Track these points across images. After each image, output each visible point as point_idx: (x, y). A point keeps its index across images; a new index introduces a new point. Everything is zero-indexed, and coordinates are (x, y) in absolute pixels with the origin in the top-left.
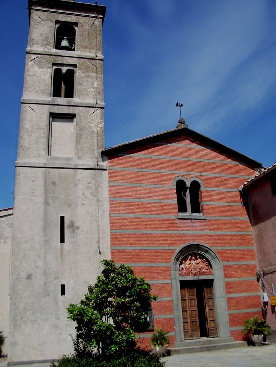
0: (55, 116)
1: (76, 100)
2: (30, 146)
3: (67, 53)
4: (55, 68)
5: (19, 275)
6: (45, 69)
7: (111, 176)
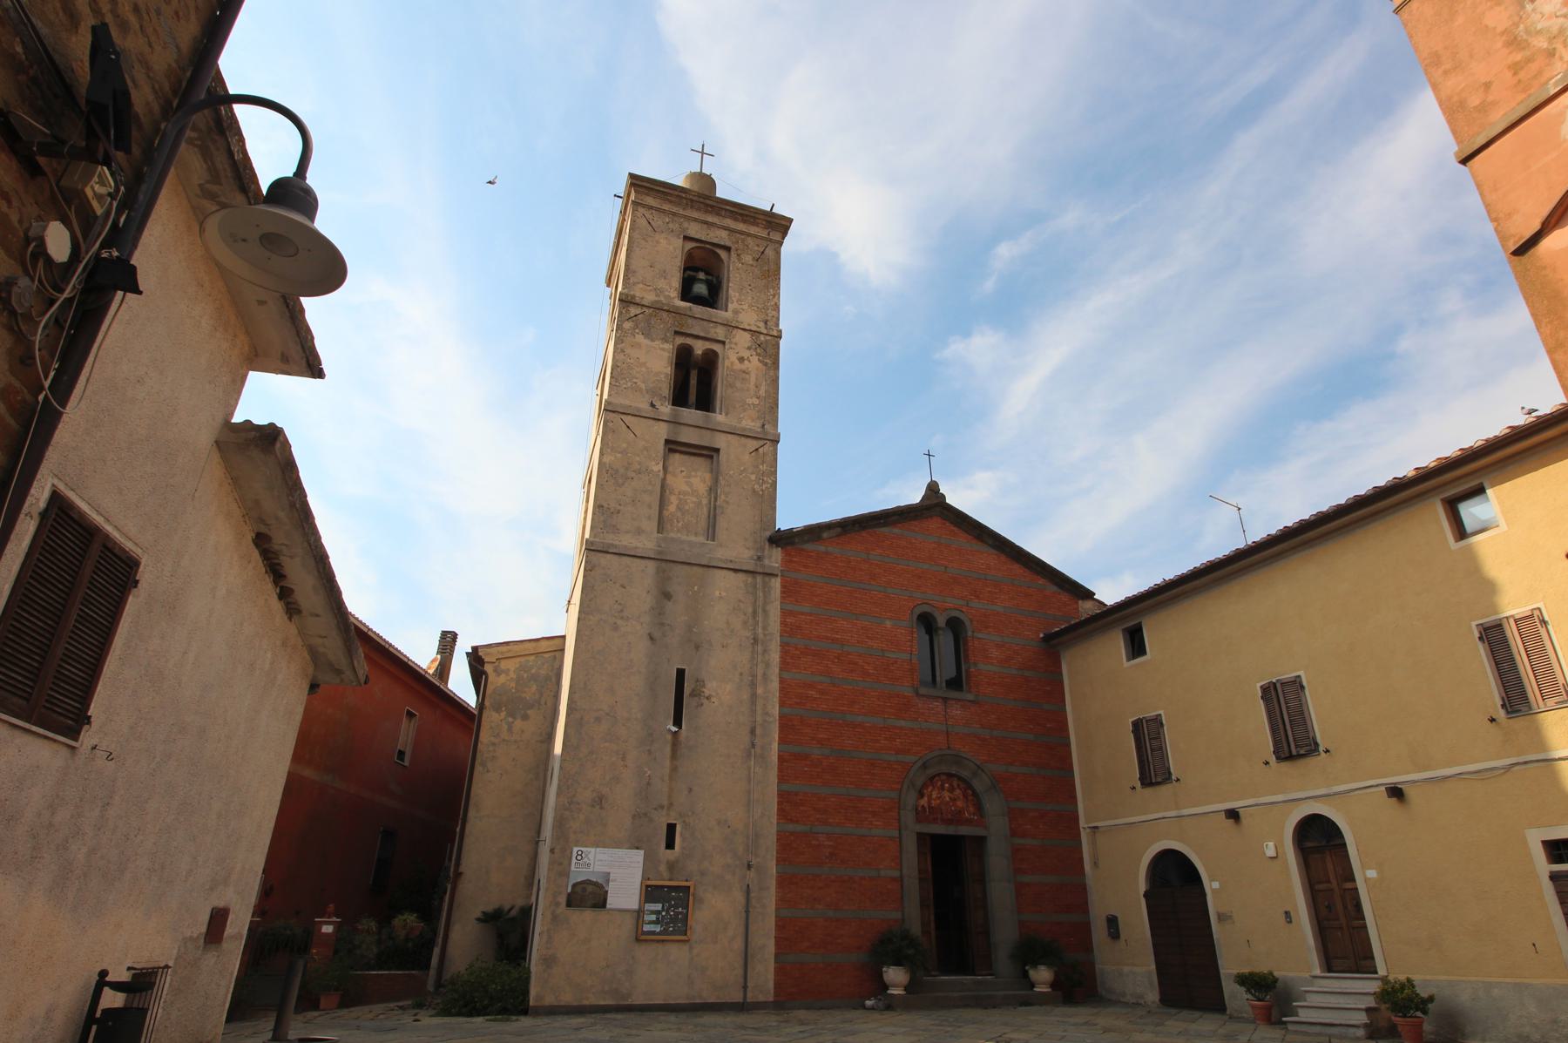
0: (672, 446)
1: (719, 418)
2: (619, 507)
3: (699, 310)
4: (680, 340)
5: (574, 796)
6: (657, 342)
7: (787, 591)
